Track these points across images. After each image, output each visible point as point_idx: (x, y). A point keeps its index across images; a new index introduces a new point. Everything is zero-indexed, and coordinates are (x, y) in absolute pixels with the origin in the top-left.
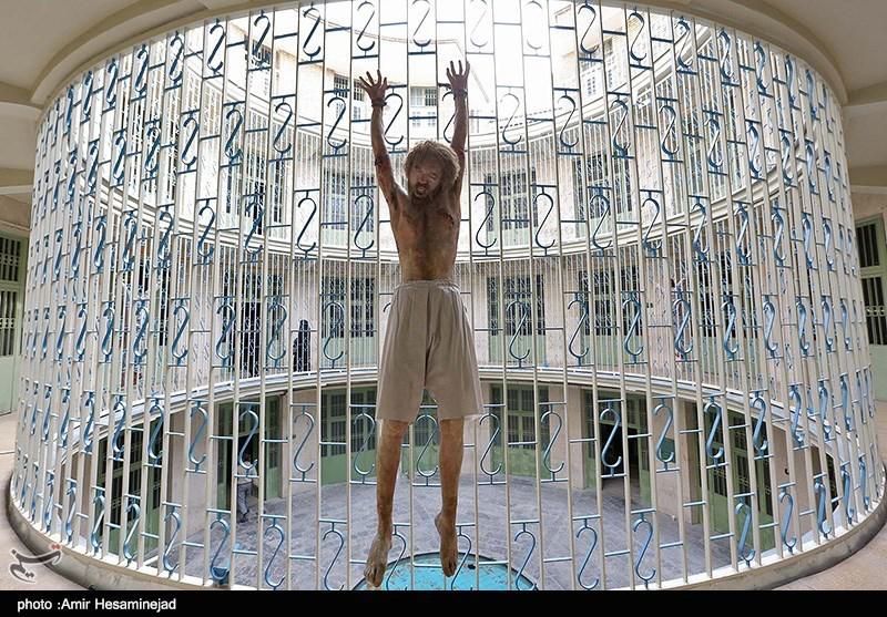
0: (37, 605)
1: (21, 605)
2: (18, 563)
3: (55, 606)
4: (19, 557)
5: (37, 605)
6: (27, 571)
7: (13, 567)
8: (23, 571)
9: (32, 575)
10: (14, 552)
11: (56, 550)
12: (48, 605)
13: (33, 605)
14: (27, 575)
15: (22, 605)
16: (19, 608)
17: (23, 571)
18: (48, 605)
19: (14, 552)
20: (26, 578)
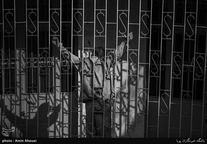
1: (3, 141)
2: (5, 132)
3: (13, 141)
4: (4, 130)
7: (3, 132)
8: (5, 133)
9: (7, 134)
10: (3, 129)
11: (13, 128)
12: (11, 141)
14: (6, 134)
15: (3, 141)
16: (3, 142)
17: (5, 133)
18: (11, 141)
19: (3, 129)
20: (6, 135)
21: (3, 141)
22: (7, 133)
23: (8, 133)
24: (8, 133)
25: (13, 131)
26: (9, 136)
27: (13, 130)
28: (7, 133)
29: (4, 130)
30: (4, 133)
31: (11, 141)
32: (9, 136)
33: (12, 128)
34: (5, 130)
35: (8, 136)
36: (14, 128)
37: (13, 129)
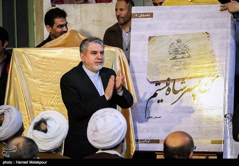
0: (8, 163)
2: (6, 152)
3: (13, 163)
4: (5, 150)
5: (8, 163)
6: (7, 154)
7: (3, 153)
8: (6, 154)
9: (8, 155)
10: (3, 149)
11: (15, 148)
12: (11, 163)
13: (7, 163)
14: (7, 155)
15: (4, 163)
16: (3, 163)
17: (6, 154)
18: (11, 163)
19: (3, 149)
21: (4, 163)
22: (8, 153)
25: (14, 151)
28: (8, 153)
29: (5, 150)
30: (4, 154)
32: (9, 157)
33: (14, 147)
34: (6, 150)
35: (9, 156)
36: (15, 147)
37: (15, 149)
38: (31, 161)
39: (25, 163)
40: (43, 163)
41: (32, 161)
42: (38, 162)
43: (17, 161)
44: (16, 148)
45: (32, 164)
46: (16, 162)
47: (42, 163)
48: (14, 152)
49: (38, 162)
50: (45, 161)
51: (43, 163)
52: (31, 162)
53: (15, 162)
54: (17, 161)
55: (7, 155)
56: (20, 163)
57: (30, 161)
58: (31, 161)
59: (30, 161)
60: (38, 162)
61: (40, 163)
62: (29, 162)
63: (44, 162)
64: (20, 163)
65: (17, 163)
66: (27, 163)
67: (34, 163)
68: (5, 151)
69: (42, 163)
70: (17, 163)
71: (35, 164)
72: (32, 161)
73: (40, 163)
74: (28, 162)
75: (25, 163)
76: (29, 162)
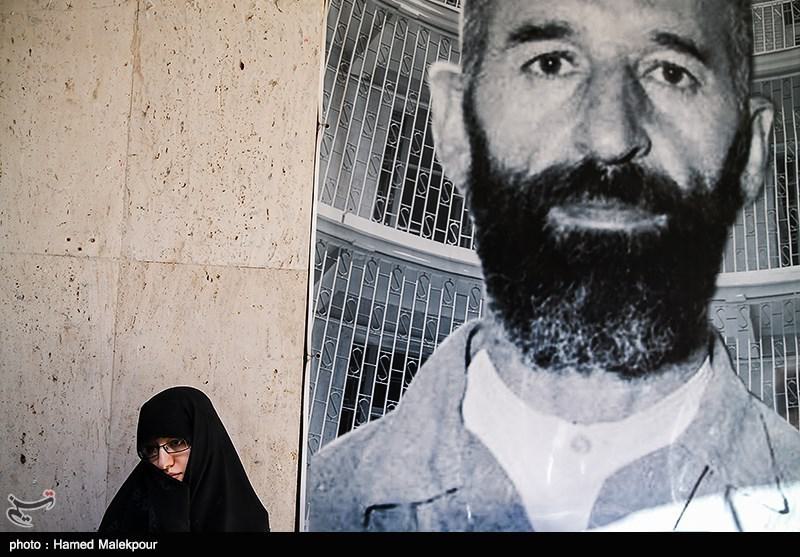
0: (27, 545)
2: (20, 509)
3: (43, 546)
4: (15, 502)
5: (27, 545)
7: (11, 512)
8: (20, 515)
9: (28, 519)
10: (12, 498)
12: (37, 545)
13: (23, 546)
14: (24, 519)
15: (14, 546)
16: (11, 548)
17: (20, 515)
18: (37, 545)
19: (12, 498)
23: (29, 513)
24: (29, 513)
26: (32, 525)
27: (50, 503)
28: (25, 513)
29: (15, 502)
30: (13, 516)
31: (34, 545)
32: (32, 525)
34: (18, 504)
36: (51, 494)
37: (51, 500)
38: (103, 542)
39: (83, 545)
40: (142, 545)
41: (107, 541)
42: (128, 545)
43: (58, 541)
44: (53, 496)
45: (107, 551)
46: (55, 544)
47: (139, 545)
48: (47, 509)
49: (126, 545)
50: (149, 541)
51: (142, 545)
52: (103, 545)
53: (52, 544)
54: (58, 541)
55: (24, 519)
56: (66, 545)
57: (100, 541)
58: (103, 542)
59: (100, 541)
60: (126, 545)
61: (135, 545)
62: (96, 544)
63: (146, 545)
64: (66, 545)
65: (58, 546)
66: (90, 545)
67: (113, 546)
68: (18, 506)
69: (139, 545)
70: (58, 546)
71: (118, 552)
72: (107, 541)
73: (135, 545)
74: (92, 542)
75: (83, 545)
76: (96, 544)
